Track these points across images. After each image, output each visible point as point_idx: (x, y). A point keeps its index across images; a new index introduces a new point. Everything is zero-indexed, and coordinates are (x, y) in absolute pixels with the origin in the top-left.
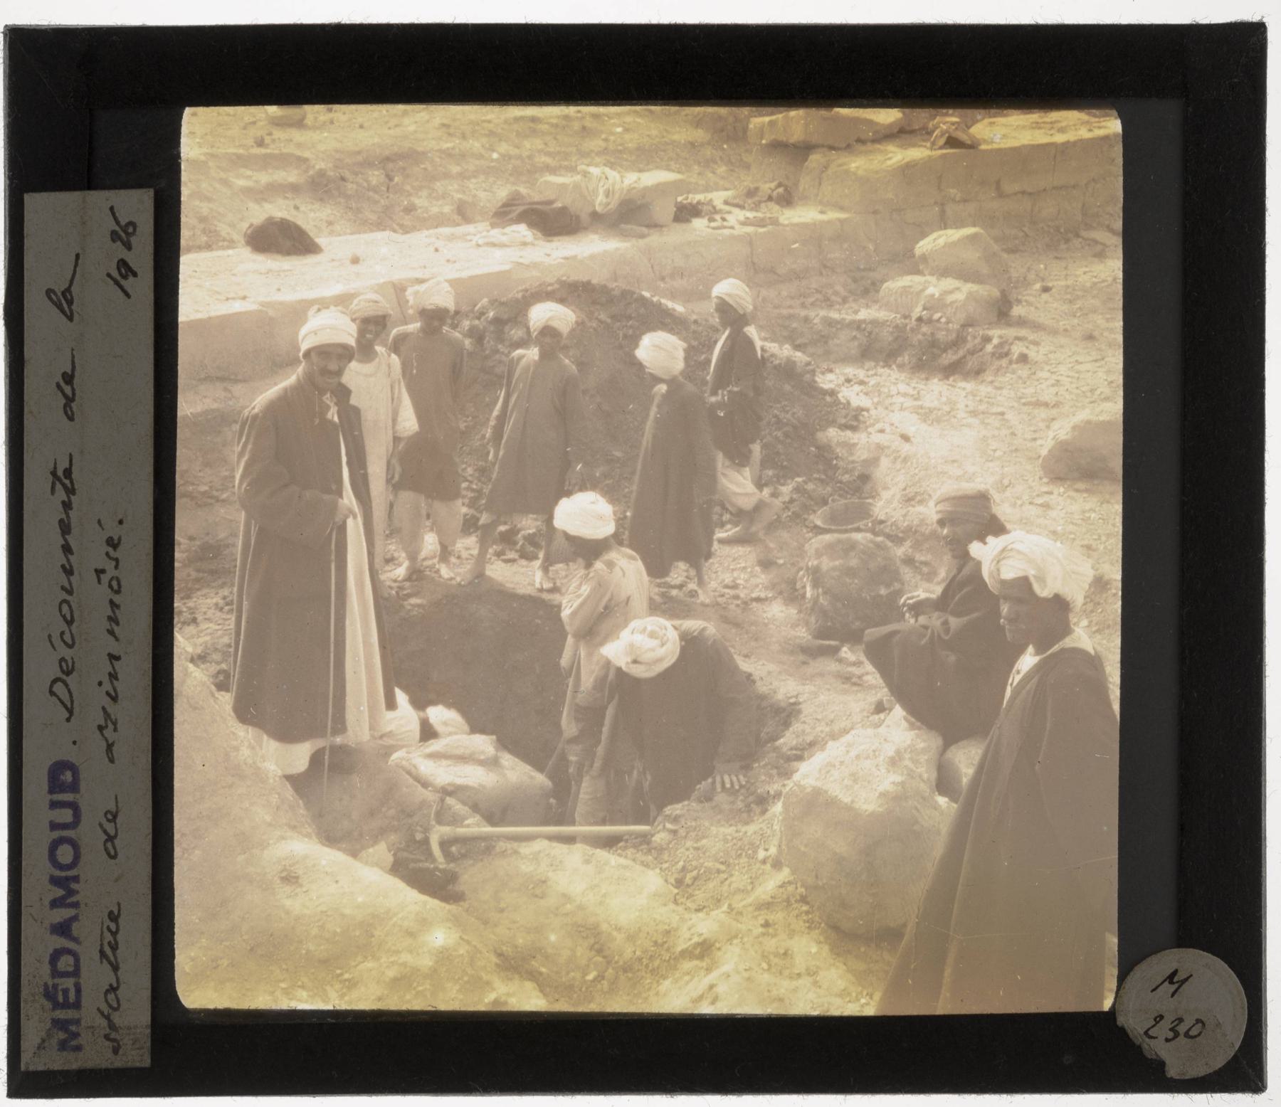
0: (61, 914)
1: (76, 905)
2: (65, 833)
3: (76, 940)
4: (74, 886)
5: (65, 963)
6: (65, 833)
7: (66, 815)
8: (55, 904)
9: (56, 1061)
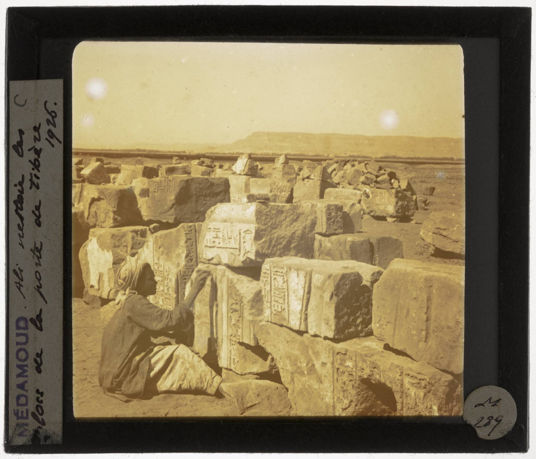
0: (21, 380)
1: (27, 376)
2: (23, 346)
3: (27, 391)
4: (26, 368)
5: (23, 400)
6: (23, 346)
7: (22, 339)
8: (19, 376)
9: (19, 441)
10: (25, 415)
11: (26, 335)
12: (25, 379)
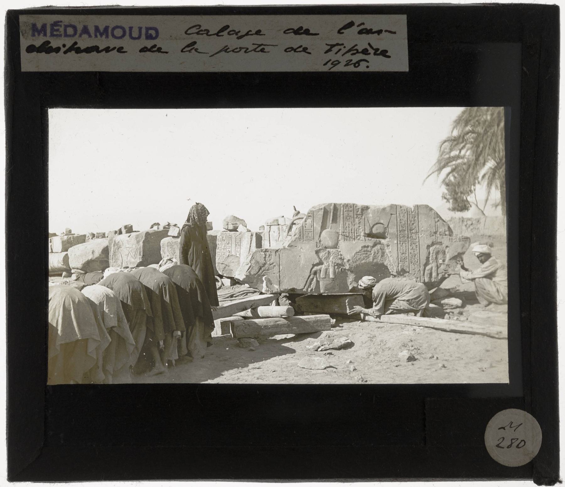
0: (92, 30)
1: (96, 36)
5: (70, 31)
7: (135, 34)
8: (97, 29)
10: (55, 33)
11: (139, 38)
12: (93, 35)
